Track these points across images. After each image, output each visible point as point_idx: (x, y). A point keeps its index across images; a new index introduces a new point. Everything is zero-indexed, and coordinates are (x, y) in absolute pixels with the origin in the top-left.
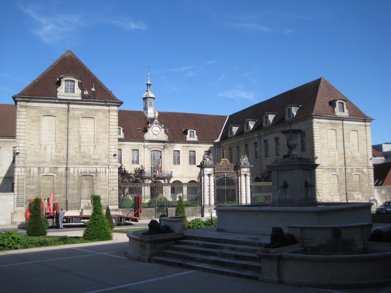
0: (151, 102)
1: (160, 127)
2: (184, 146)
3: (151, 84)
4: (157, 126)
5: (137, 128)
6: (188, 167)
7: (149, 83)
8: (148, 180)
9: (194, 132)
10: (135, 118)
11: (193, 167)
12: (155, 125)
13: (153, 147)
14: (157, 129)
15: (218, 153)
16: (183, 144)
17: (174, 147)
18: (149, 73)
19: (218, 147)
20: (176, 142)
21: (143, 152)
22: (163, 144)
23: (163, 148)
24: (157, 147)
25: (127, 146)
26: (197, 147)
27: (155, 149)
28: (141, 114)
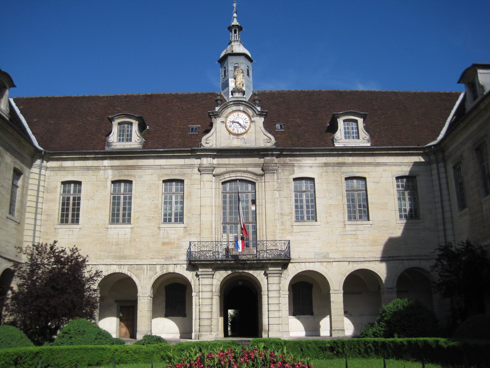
0: (237, 65)
1: (250, 112)
2: (326, 165)
3: (240, 28)
4: (240, 111)
5: (190, 126)
6: (345, 227)
7: (235, 22)
8: (211, 270)
9: (356, 121)
10: (192, 106)
11: (361, 227)
12: (234, 108)
13: (229, 169)
14: (242, 118)
15: (439, 179)
16: (325, 158)
18: (235, 5)
19: (438, 163)
20: (300, 150)
21: (195, 186)
22: (261, 161)
23: (259, 171)
24: (239, 169)
25: (150, 171)
26: (369, 164)
27: (233, 176)
28: (211, 98)
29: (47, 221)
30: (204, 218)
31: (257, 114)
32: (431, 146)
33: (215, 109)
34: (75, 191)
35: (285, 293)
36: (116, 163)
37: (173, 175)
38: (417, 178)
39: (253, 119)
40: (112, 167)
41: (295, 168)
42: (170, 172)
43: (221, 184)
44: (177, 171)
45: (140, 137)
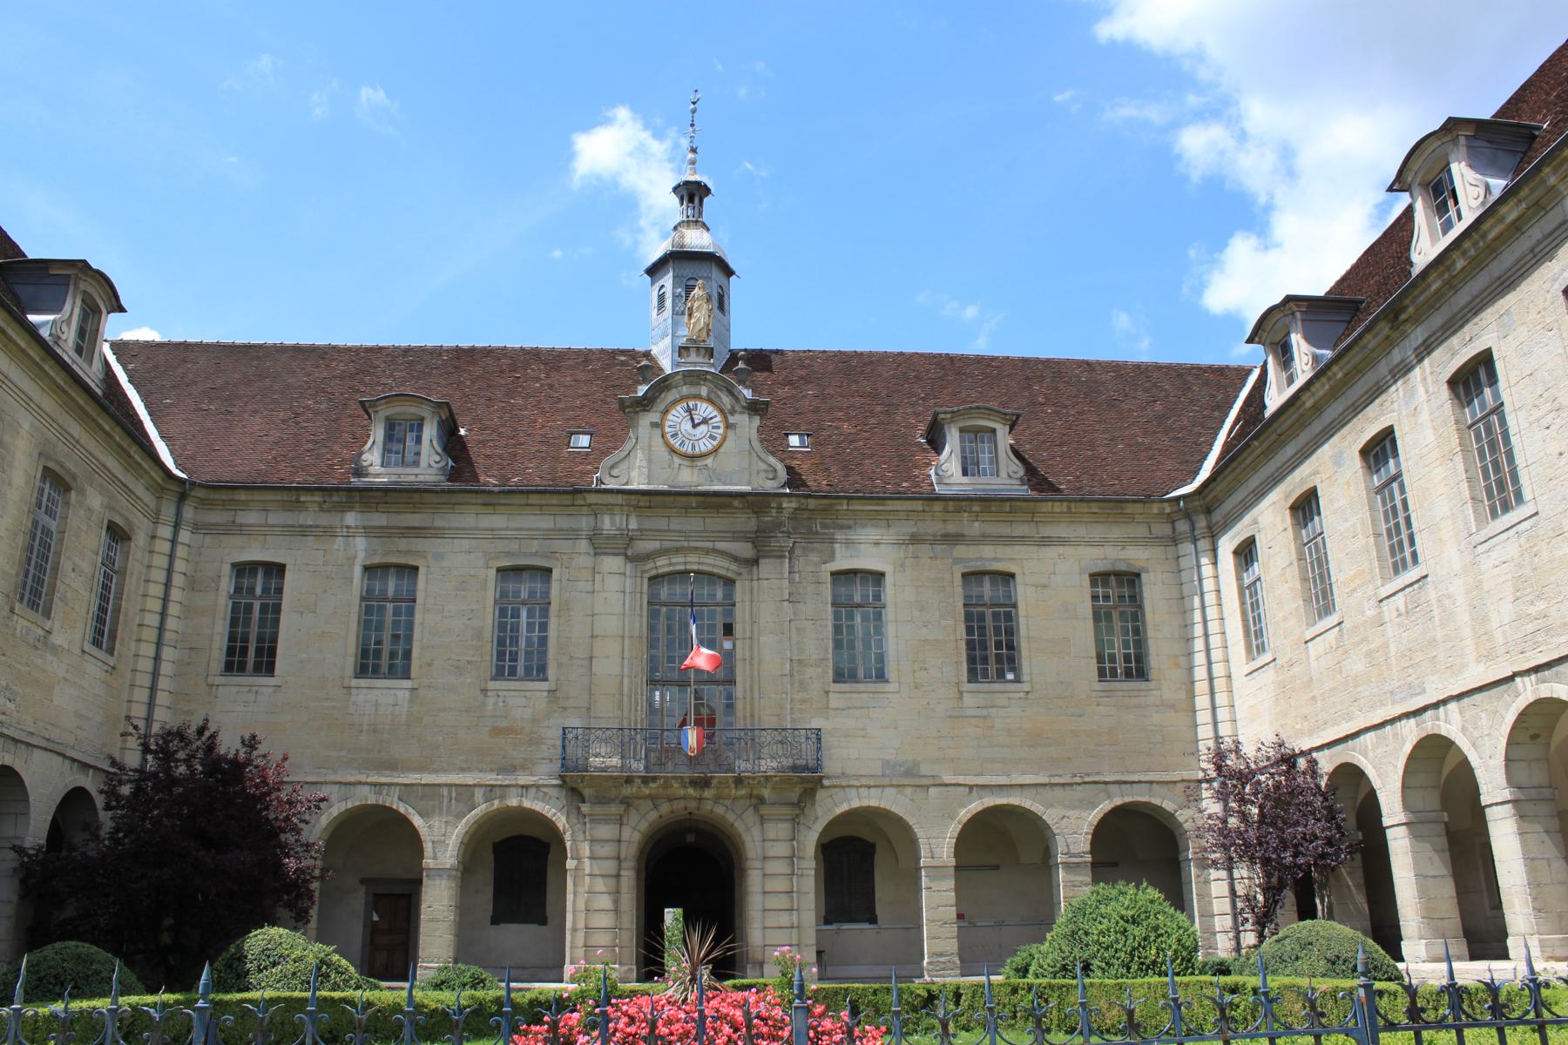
1: (726, 400)
2: (915, 540)
6: (961, 698)
10: (576, 381)
11: (1001, 700)
12: (685, 390)
17: (837, 546)
21: (581, 585)
24: (693, 544)
25: (466, 544)
27: (679, 563)
28: (623, 363)
29: (189, 664)
30: (600, 667)
31: (744, 407)
32: (1178, 499)
33: (636, 393)
34: (265, 590)
35: (809, 864)
36: (379, 519)
37: (525, 554)
38: (1144, 576)
39: (732, 419)
40: (368, 531)
41: (837, 546)
42: (517, 547)
43: (646, 581)
44: (534, 546)
45: (438, 453)
